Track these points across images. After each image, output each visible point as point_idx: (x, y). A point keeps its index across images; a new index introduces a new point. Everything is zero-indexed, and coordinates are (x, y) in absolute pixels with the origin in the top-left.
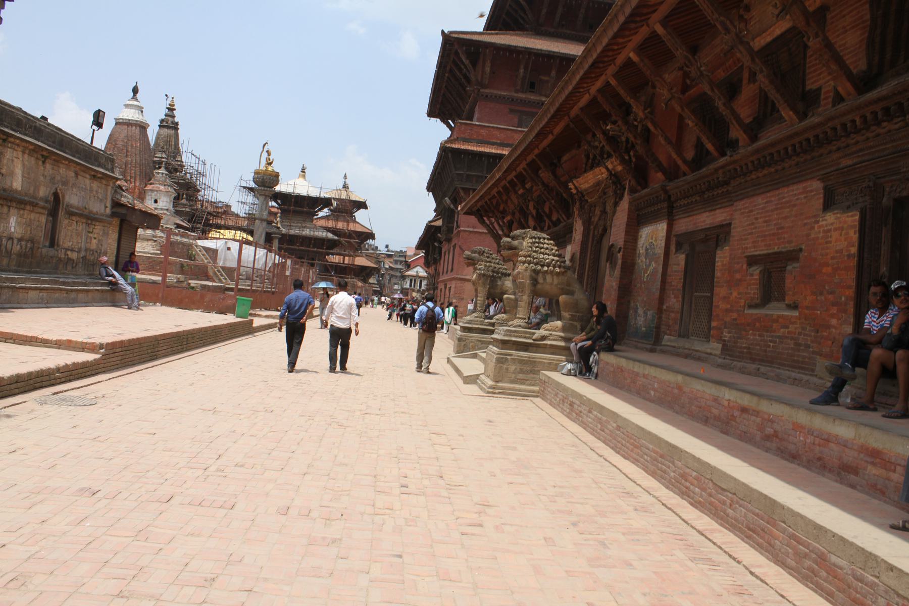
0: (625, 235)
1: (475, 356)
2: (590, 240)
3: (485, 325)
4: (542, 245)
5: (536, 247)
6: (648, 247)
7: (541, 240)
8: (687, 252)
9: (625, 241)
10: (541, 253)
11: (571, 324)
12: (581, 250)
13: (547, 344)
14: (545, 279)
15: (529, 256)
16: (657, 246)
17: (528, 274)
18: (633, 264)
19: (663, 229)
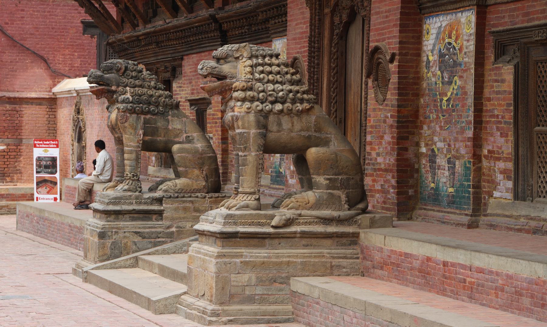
0: (400, 32)
1: (135, 263)
2: (327, 34)
3: (145, 203)
4: (268, 69)
5: (262, 72)
6: (444, 51)
7: (267, 60)
8: (515, 61)
9: (400, 43)
10: (269, 81)
11: (329, 193)
12: (310, 52)
13: (295, 233)
14: (279, 124)
15: (251, 89)
16: (461, 49)
17: (252, 117)
18: (418, 79)
19: (470, 22)
